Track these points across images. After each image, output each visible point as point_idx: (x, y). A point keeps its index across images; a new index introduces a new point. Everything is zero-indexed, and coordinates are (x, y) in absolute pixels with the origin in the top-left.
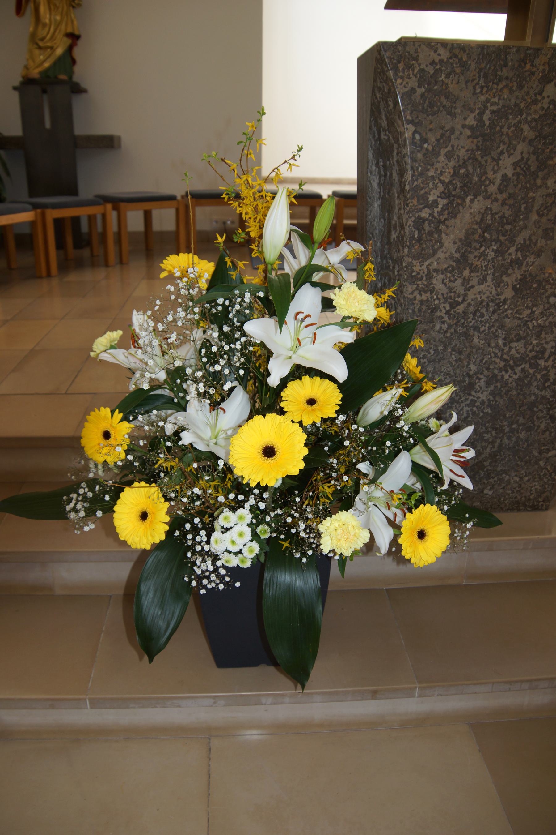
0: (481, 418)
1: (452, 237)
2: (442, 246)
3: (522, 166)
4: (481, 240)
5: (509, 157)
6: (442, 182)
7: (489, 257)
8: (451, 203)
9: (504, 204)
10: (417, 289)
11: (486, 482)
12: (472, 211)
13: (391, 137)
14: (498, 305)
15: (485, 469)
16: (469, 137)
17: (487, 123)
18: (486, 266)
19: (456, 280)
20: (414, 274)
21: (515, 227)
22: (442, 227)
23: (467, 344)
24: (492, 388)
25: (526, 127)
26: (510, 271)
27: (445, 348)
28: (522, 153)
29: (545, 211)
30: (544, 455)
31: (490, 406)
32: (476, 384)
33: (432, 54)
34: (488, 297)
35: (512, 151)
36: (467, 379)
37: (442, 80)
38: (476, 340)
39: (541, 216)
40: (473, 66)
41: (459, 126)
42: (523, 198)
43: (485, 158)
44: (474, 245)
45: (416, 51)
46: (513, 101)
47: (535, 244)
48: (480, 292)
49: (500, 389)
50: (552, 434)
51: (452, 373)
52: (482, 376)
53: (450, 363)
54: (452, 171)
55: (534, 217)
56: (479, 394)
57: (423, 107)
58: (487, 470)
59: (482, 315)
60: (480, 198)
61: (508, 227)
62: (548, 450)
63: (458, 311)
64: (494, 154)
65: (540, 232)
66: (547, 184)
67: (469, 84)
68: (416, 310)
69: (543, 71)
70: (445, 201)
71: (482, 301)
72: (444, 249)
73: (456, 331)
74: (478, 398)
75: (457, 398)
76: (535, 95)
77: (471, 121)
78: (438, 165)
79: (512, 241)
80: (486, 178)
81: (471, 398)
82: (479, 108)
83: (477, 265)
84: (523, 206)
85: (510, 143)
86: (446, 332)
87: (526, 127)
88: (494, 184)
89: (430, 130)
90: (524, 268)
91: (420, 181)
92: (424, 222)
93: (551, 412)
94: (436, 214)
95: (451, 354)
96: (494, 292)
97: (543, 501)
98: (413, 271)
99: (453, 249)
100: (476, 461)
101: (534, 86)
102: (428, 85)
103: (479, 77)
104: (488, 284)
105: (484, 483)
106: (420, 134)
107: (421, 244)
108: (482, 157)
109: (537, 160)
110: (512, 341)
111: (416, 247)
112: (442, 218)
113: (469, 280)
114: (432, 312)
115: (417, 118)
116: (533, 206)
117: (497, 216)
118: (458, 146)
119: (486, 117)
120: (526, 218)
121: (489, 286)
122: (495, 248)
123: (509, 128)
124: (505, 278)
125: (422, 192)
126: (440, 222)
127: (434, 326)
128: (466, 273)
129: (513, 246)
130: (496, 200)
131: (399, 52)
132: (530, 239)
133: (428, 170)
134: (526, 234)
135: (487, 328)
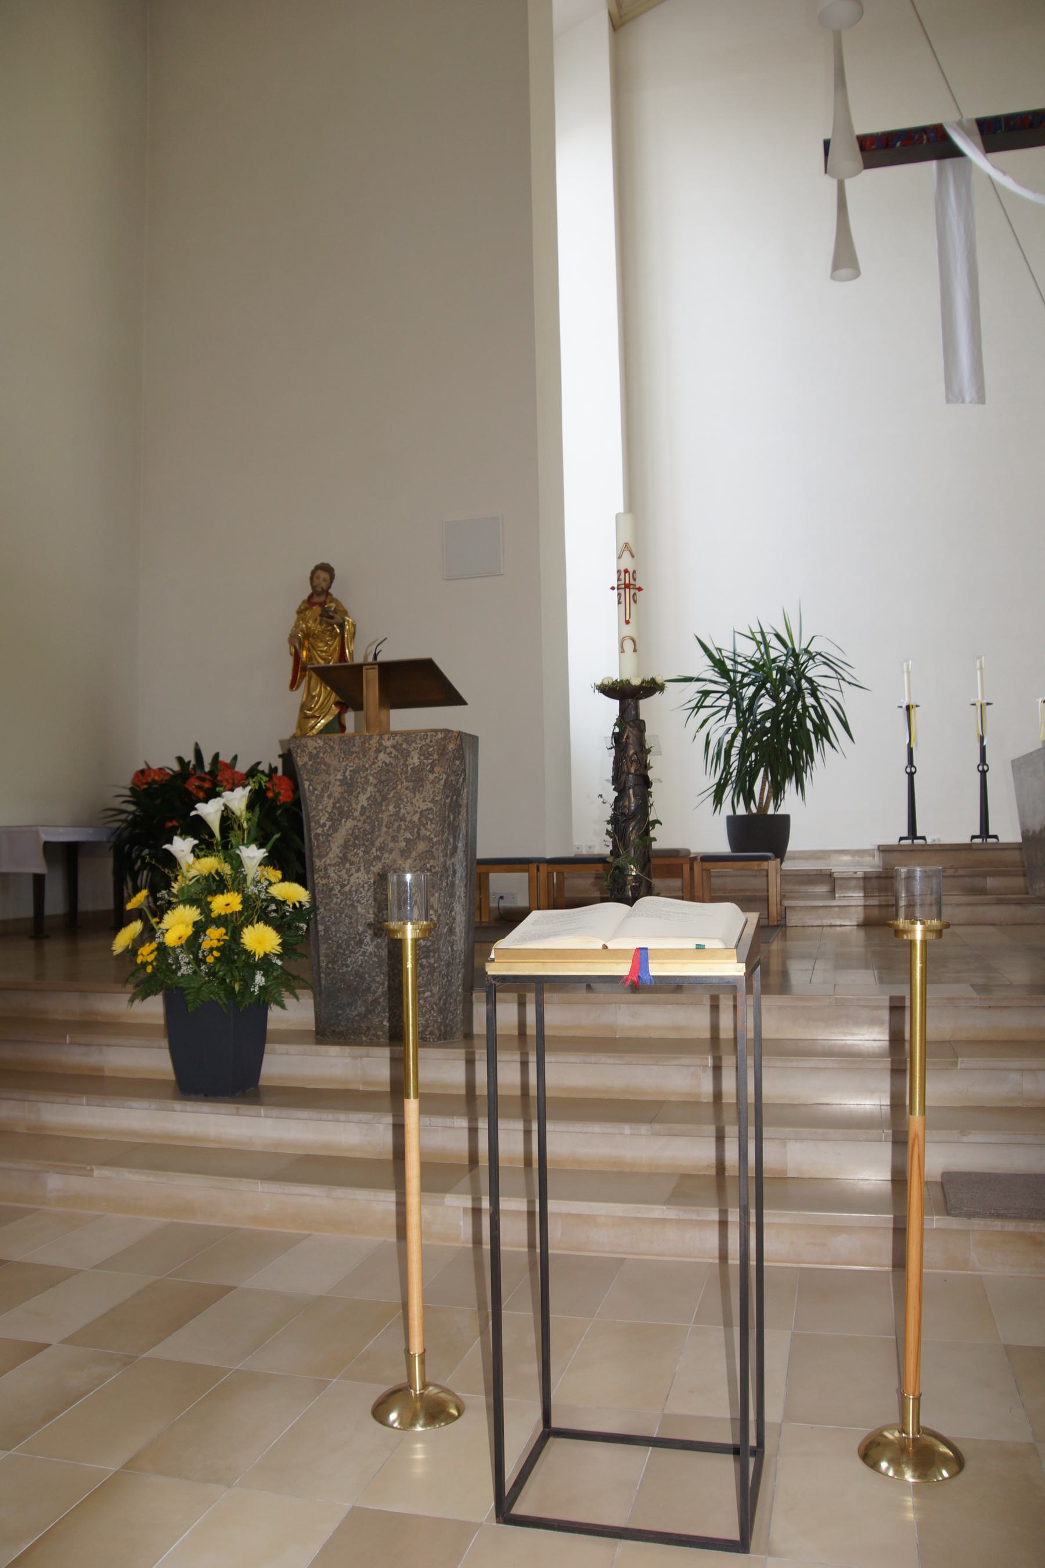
0: (371, 964)
1: (337, 844)
2: (331, 850)
4: (354, 845)
6: (327, 812)
7: (360, 855)
8: (333, 823)
9: (364, 822)
10: (319, 876)
11: (383, 1015)
12: (346, 828)
14: (369, 885)
15: (381, 1005)
16: (339, 786)
17: (349, 777)
18: (359, 861)
19: (342, 870)
20: (317, 867)
21: (373, 836)
22: (330, 838)
23: (355, 912)
24: (375, 943)
25: (371, 778)
26: (374, 864)
27: (341, 916)
28: (371, 792)
29: (391, 825)
30: (422, 995)
31: (375, 956)
32: (364, 940)
34: (363, 881)
36: (358, 936)
38: (359, 909)
39: (389, 828)
40: (337, 747)
41: (333, 781)
42: (375, 818)
43: (350, 797)
44: (350, 848)
45: (306, 743)
46: (361, 764)
47: (388, 845)
48: (358, 878)
49: (380, 944)
50: (425, 979)
51: (347, 932)
52: (366, 934)
53: (346, 925)
54: (332, 805)
55: (384, 829)
56: (367, 947)
58: (383, 1005)
59: (361, 893)
60: (350, 820)
61: (369, 836)
62: (424, 992)
63: (346, 890)
64: (355, 794)
65: (389, 838)
68: (320, 890)
69: (376, 747)
70: (330, 823)
71: (359, 884)
72: (333, 851)
73: (346, 904)
74: (367, 950)
75: (353, 950)
77: (339, 777)
78: (325, 802)
79: (373, 844)
80: (352, 808)
81: (362, 950)
83: (353, 861)
84: (376, 823)
85: (363, 786)
86: (340, 904)
87: (371, 778)
88: (357, 811)
89: (318, 783)
90: (383, 862)
91: (315, 812)
92: (319, 836)
93: (420, 962)
94: (325, 831)
95: (345, 919)
96: (366, 878)
97: (430, 1034)
98: (316, 866)
99: (338, 851)
100: (374, 998)
103: (341, 753)
104: (362, 872)
105: (382, 1016)
107: (319, 849)
109: (380, 795)
110: (383, 910)
111: (316, 851)
112: (330, 833)
113: (349, 871)
114: (330, 891)
115: (310, 777)
116: (382, 823)
117: (361, 830)
119: (347, 774)
120: (380, 830)
121: (362, 874)
122: (363, 849)
123: (361, 778)
124: (371, 868)
125: (317, 818)
126: (329, 835)
127: (332, 900)
128: (347, 866)
129: (374, 847)
130: (360, 820)
132: (383, 842)
133: (318, 806)
134: (381, 840)
135: (365, 901)
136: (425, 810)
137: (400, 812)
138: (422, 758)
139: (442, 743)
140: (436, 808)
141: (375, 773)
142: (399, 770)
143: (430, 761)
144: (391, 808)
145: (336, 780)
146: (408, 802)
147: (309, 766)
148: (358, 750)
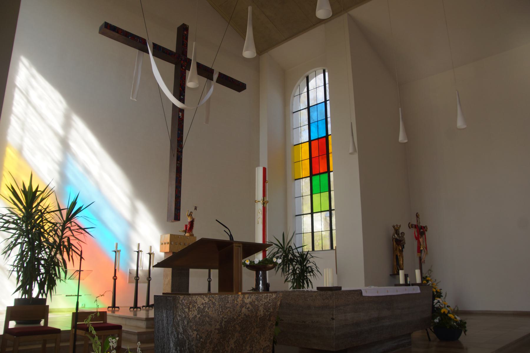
3: (237, 342)
5: (232, 340)
13: (184, 337)
17: (224, 326)
25: (237, 326)
28: (237, 337)
33: (202, 300)
35: (233, 337)
37: (206, 311)
57: (200, 323)
66: (246, 349)
67: (216, 311)
76: (239, 312)
80: (225, 350)
82: (220, 321)
87: (237, 326)
89: (203, 333)
101: (238, 309)
102: (201, 313)
103: (219, 308)
106: (199, 335)
108: (223, 342)
115: (198, 328)
118: (214, 338)
119: (223, 324)
131: (190, 300)
136: (266, 347)
137: (253, 350)
138: (265, 311)
139: (275, 301)
140: (271, 345)
141: (240, 322)
142: (253, 320)
143: (269, 313)
144: (248, 348)
145: (215, 329)
146: (257, 342)
147: (197, 319)
148: (230, 306)
